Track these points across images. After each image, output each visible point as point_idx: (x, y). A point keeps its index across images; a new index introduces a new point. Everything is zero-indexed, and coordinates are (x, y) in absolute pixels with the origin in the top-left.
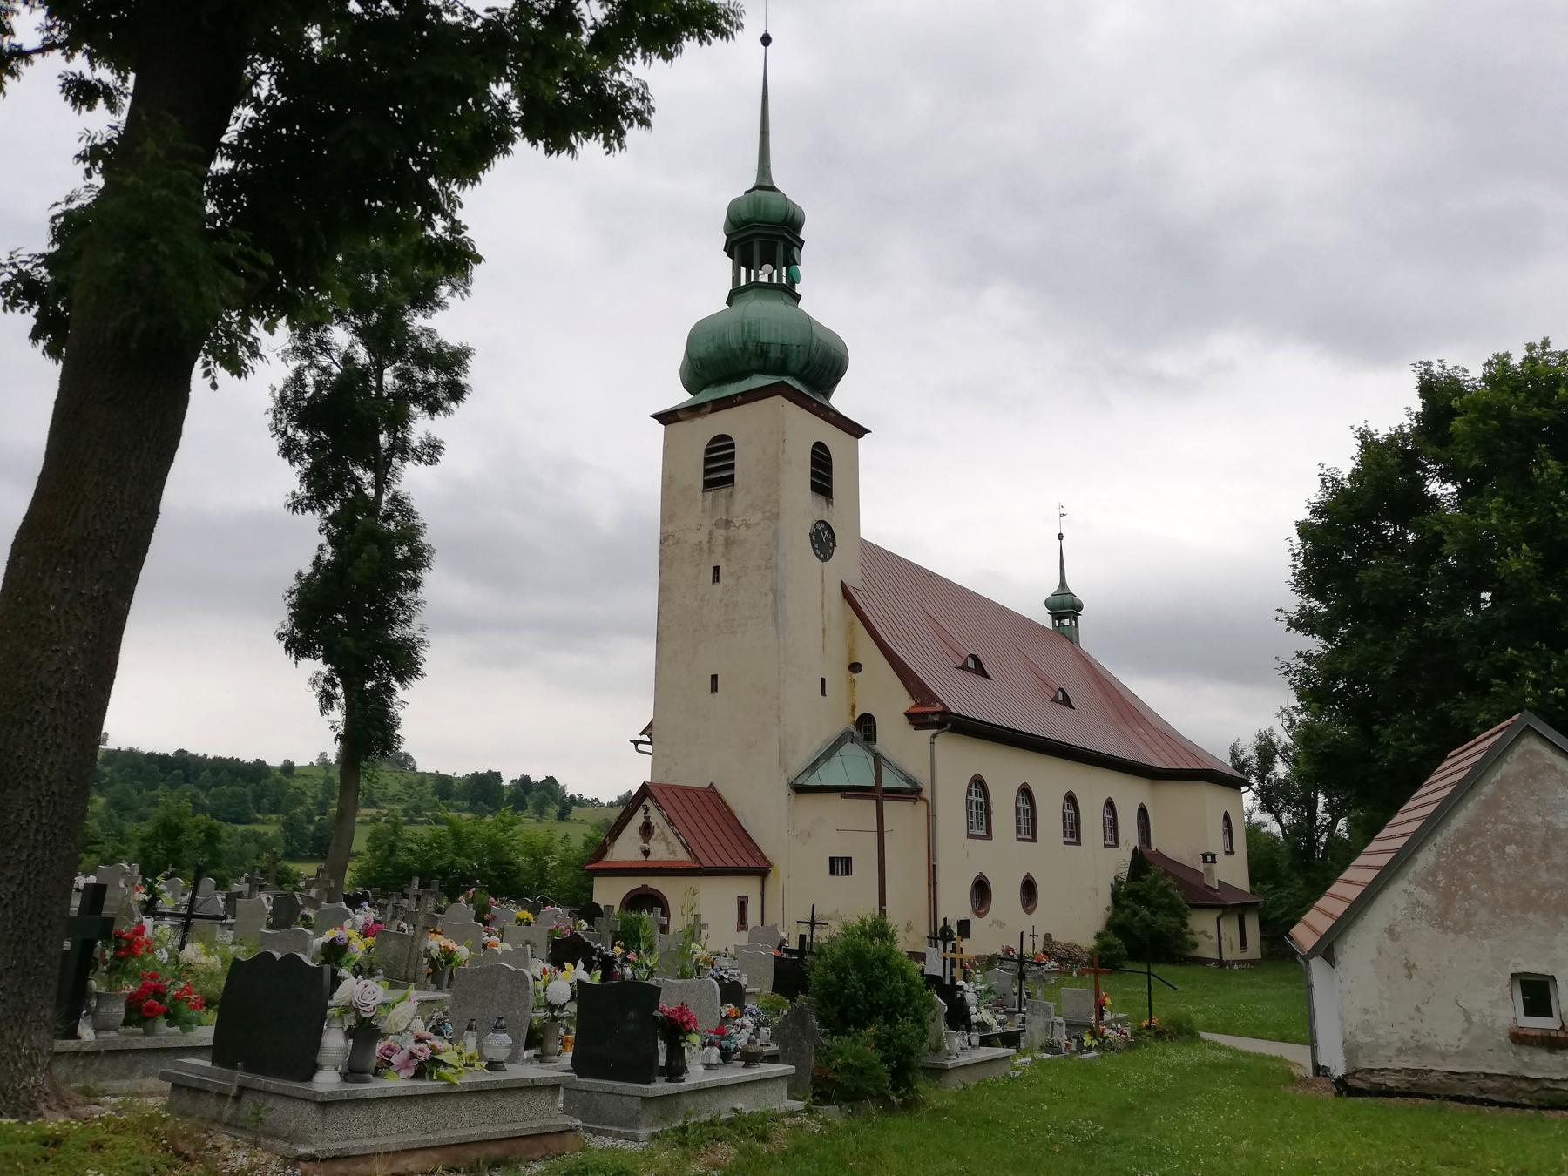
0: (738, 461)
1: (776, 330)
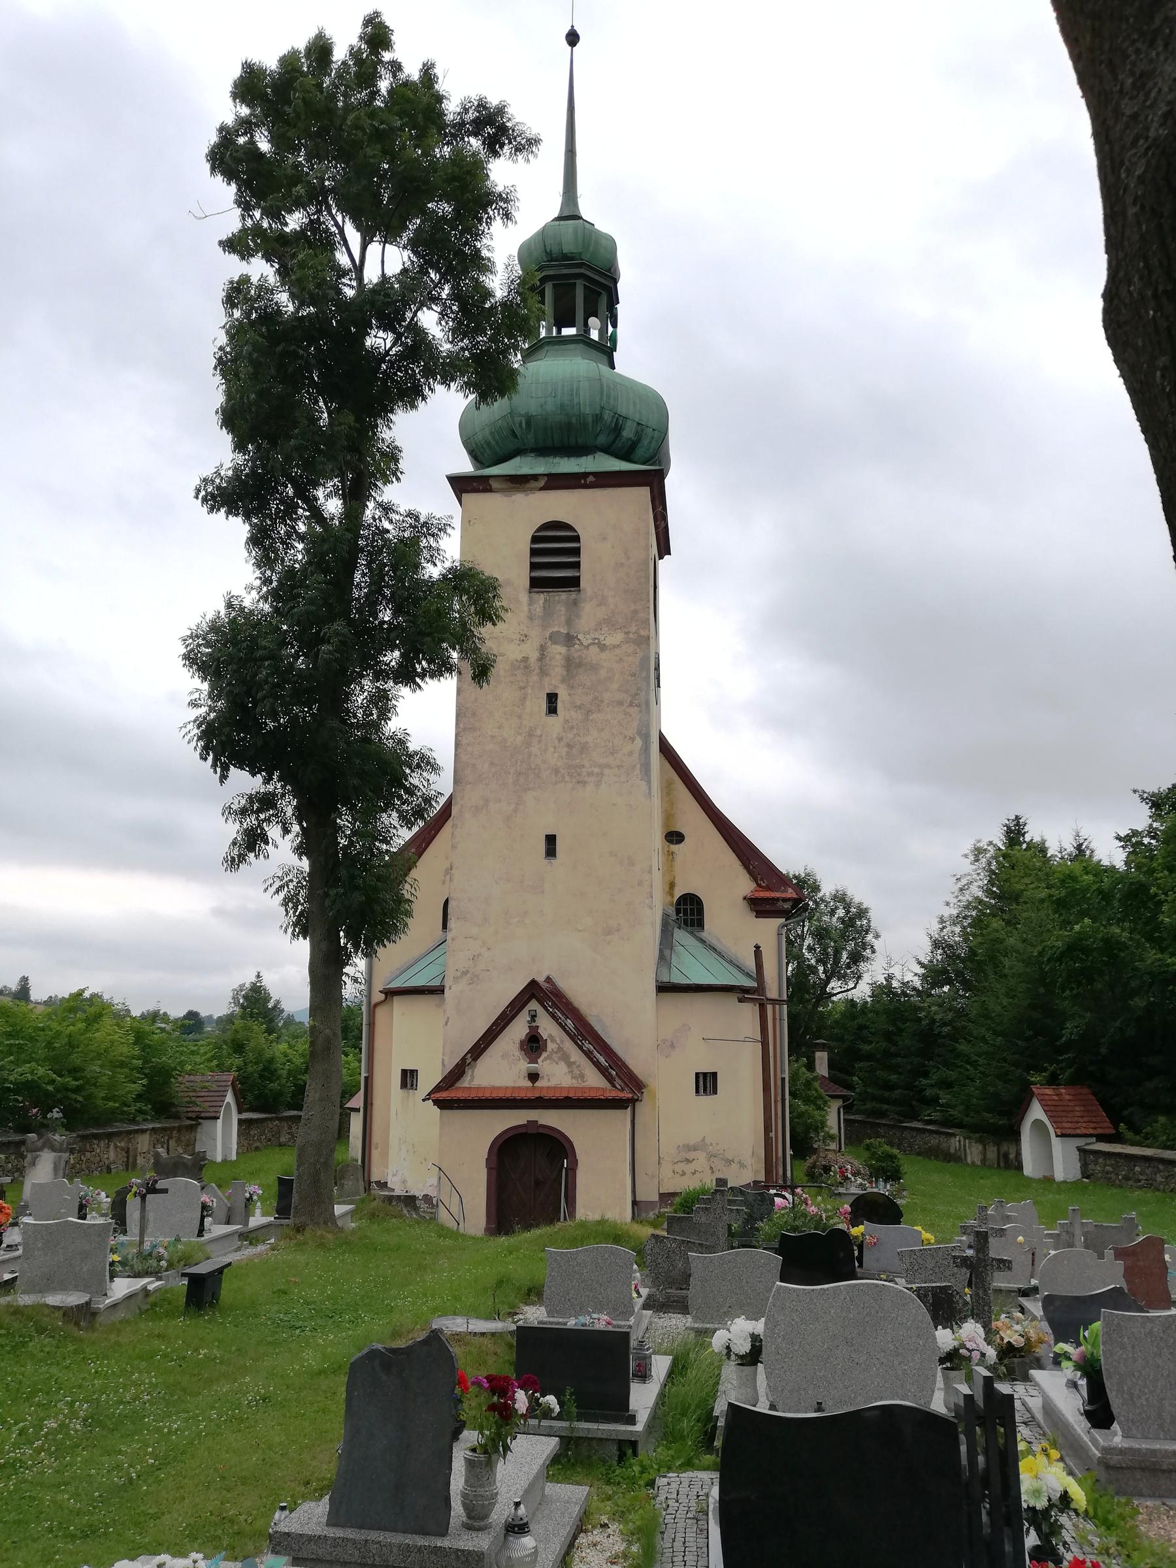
0: (584, 559)
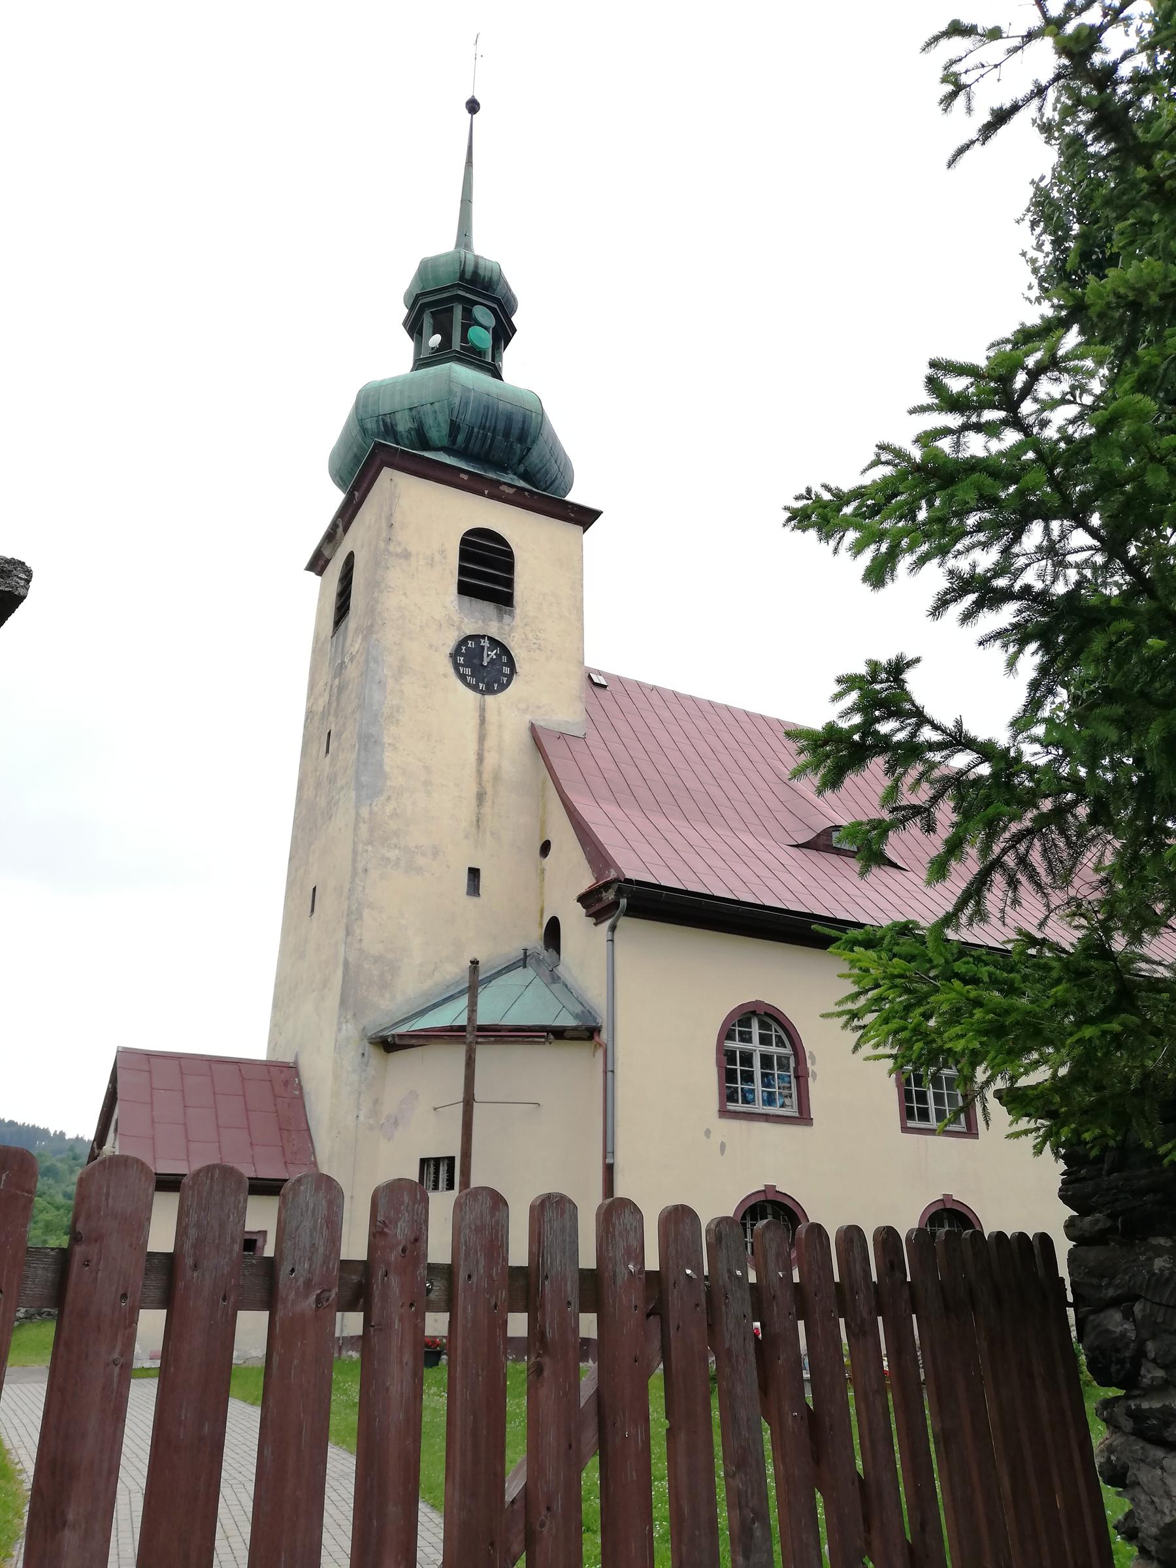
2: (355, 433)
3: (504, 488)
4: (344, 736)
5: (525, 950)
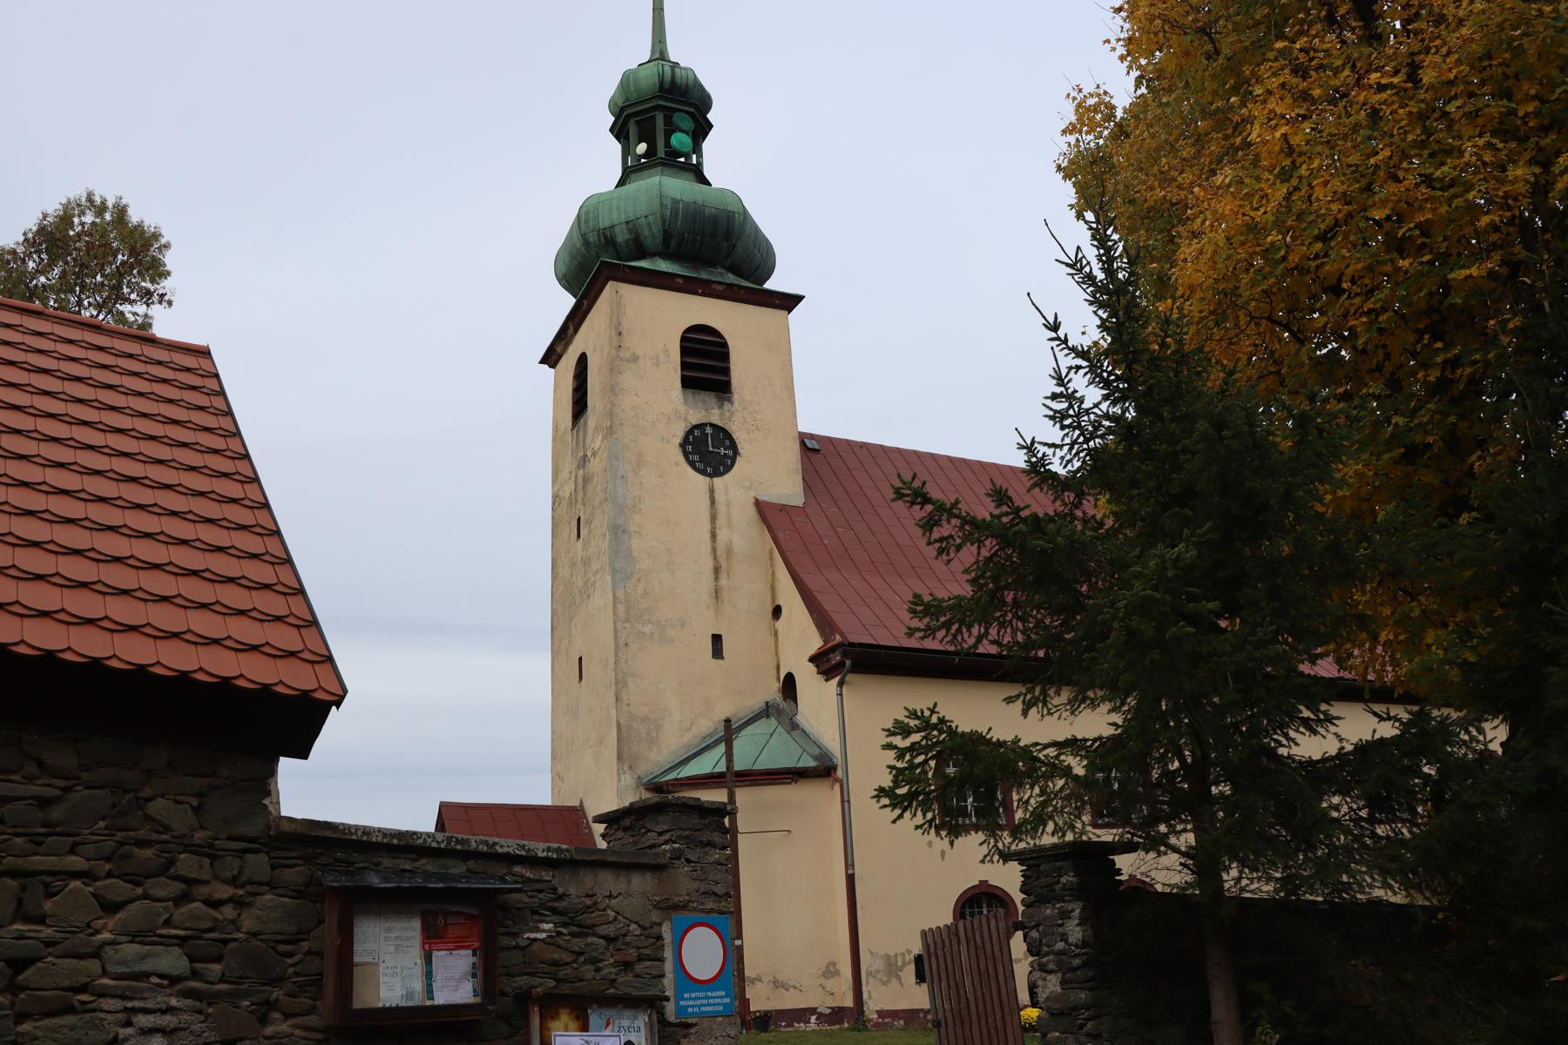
1: (618, 208)
2: (579, 245)
3: (714, 286)
4: (594, 524)
5: (767, 703)
